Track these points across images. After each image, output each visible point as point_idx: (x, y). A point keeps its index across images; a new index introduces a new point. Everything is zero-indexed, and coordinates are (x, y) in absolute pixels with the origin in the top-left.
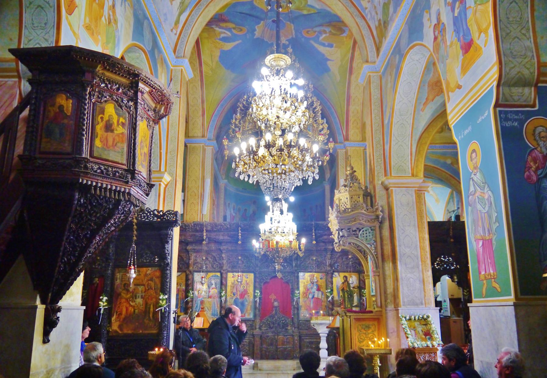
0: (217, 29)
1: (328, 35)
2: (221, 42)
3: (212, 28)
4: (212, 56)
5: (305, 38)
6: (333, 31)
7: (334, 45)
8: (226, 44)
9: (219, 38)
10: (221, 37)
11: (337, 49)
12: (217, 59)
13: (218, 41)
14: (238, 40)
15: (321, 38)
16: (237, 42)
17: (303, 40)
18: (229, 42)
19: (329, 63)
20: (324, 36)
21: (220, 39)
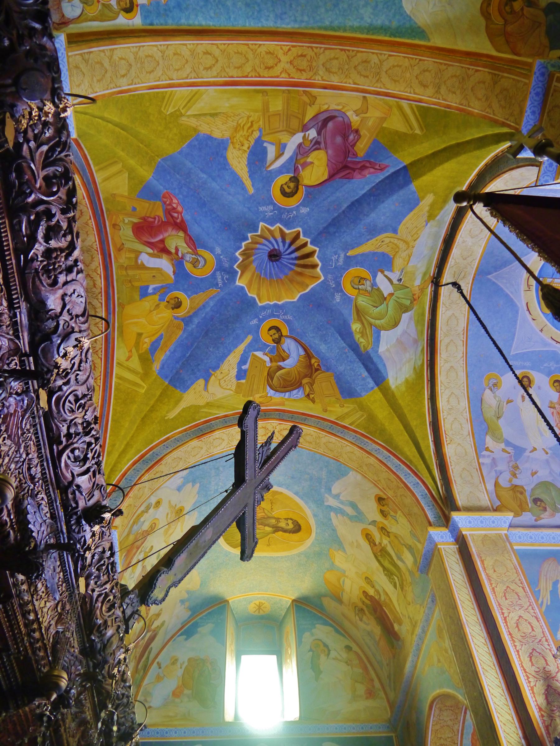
0: (298, 138)
1: (268, 364)
2: (252, 143)
3: (305, 128)
4: (213, 115)
5: (258, 327)
6: (280, 372)
7: (243, 381)
8: (246, 155)
9: (263, 139)
10: (265, 145)
11: (234, 388)
12: (205, 128)
13: (256, 134)
14: (253, 186)
15: (259, 354)
16: (248, 183)
17: (255, 321)
19: (201, 382)
20: (267, 359)
21: (259, 142)
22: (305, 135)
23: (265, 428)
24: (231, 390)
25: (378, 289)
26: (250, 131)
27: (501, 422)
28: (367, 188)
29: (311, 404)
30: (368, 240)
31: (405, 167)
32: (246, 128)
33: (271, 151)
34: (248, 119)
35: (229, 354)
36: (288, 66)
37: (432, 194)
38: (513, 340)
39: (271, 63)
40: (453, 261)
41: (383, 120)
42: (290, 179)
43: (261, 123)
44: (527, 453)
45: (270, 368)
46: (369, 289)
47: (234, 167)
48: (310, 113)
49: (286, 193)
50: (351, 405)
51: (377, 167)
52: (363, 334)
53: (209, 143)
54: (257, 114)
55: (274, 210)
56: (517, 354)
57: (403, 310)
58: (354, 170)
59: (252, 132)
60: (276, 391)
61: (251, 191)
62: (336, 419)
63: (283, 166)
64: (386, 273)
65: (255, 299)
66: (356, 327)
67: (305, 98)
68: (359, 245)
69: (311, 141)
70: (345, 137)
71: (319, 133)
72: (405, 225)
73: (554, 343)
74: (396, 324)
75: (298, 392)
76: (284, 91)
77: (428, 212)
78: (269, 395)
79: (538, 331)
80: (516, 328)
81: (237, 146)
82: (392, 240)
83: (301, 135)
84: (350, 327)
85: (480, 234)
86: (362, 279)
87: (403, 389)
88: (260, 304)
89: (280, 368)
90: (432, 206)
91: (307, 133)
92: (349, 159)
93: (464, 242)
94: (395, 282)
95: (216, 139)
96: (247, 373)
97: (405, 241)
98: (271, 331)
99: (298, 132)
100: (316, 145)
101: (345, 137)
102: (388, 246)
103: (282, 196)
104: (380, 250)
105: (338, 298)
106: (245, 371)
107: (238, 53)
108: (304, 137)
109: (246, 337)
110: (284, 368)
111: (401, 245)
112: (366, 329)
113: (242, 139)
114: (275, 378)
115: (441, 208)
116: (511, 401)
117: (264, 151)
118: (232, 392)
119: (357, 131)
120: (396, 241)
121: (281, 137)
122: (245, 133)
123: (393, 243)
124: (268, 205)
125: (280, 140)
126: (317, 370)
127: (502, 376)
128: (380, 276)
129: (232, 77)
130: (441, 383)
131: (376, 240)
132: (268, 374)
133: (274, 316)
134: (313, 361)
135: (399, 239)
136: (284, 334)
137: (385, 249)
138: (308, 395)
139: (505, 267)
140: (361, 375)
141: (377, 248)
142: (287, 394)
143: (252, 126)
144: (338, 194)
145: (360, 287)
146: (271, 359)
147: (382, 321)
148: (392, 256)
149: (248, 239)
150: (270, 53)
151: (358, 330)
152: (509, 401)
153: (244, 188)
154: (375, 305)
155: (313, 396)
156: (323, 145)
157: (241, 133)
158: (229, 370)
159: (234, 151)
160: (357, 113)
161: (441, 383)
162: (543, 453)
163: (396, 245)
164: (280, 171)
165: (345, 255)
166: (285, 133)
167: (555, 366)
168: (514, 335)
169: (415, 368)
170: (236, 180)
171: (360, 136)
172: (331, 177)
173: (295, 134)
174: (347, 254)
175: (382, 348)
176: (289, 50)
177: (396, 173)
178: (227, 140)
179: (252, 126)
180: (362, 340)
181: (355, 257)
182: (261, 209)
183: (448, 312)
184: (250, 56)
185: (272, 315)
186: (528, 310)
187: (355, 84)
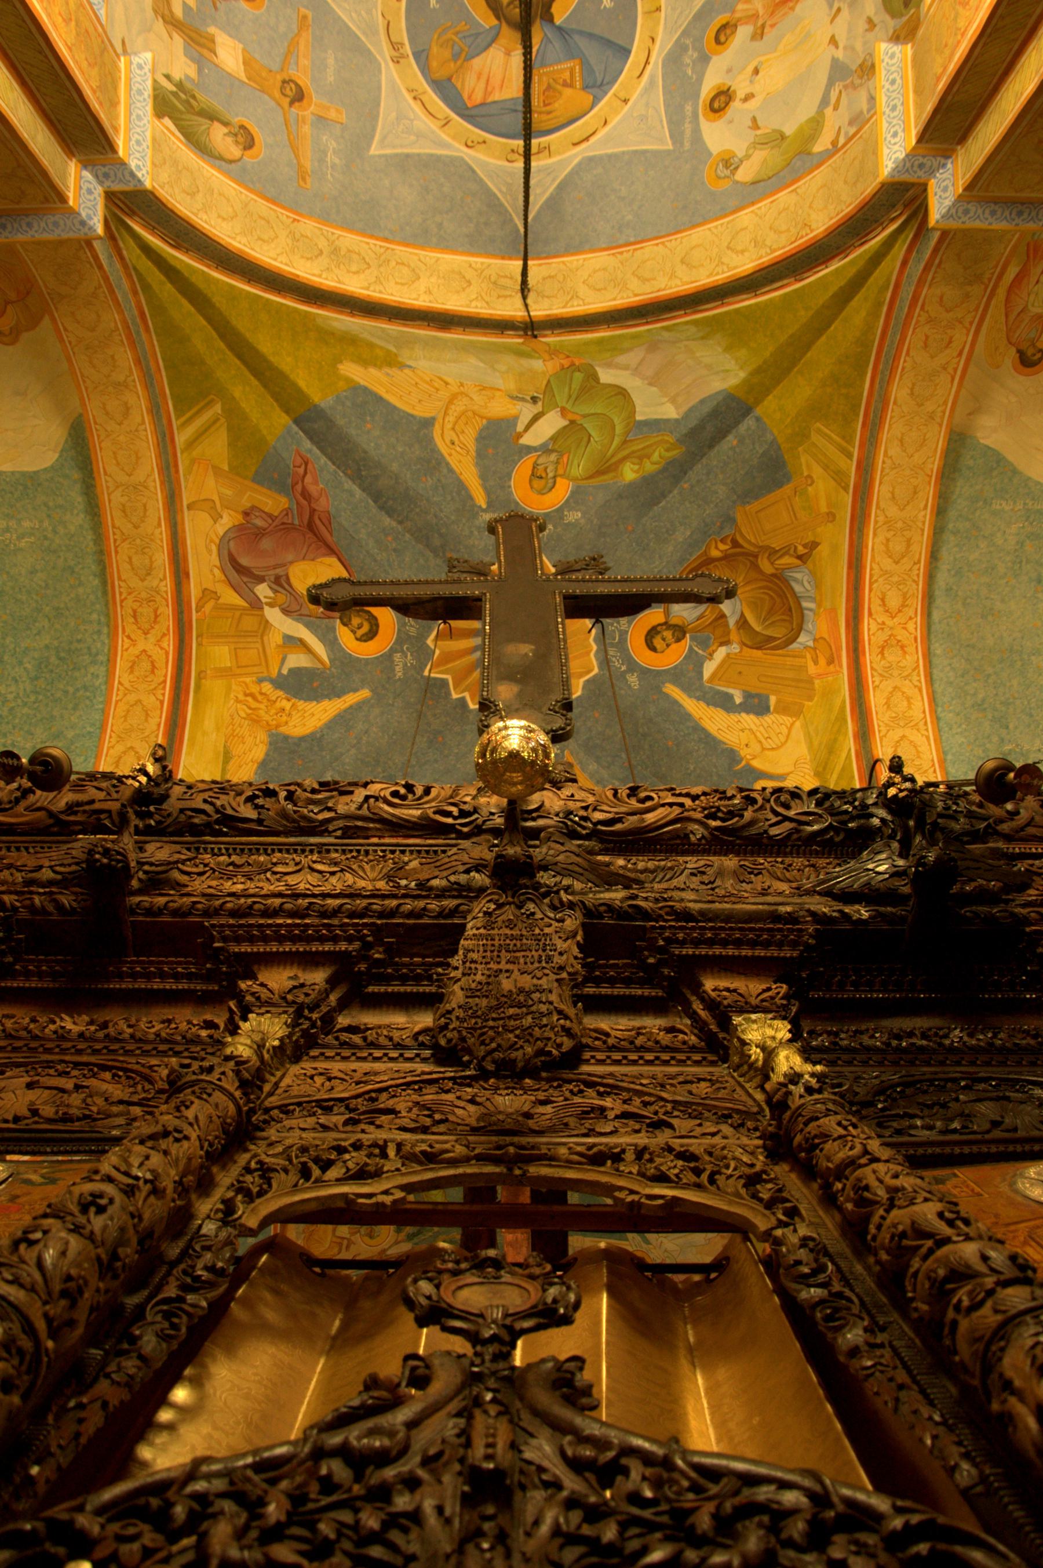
0: (273, 615)
1: (735, 648)
2: (280, 693)
3: (256, 605)
5: (645, 673)
7: (773, 700)
8: (301, 704)
9: (274, 673)
10: (285, 672)
11: (787, 720)
13: (267, 687)
14: (356, 690)
15: (709, 668)
16: (351, 699)
17: (633, 680)
18: (316, 696)
20: (721, 653)
21: (280, 683)
22: (267, 604)
23: (883, 648)
24: (792, 725)
25: (554, 438)
26: (260, 697)
27: (789, 130)
28: (348, 484)
29: (823, 550)
30: (451, 471)
31: (297, 421)
32: (254, 704)
33: (297, 660)
34: (240, 702)
35: (704, 730)
36: (152, 638)
37: (340, 367)
38: (644, 152)
39: (146, 665)
40: (474, 304)
41: (217, 471)
42: (345, 625)
43: (248, 680)
44: (840, 54)
45: (743, 644)
46: (553, 457)
47: (319, 724)
48: (230, 597)
49: (370, 631)
50: (803, 460)
51: (301, 470)
52: (641, 457)
53: (272, 765)
54: (234, 687)
55: (402, 651)
56: (671, 137)
57: (594, 383)
58: (313, 511)
59: (261, 694)
60: (800, 629)
61: (365, 693)
62: (846, 489)
63: (322, 639)
64: (520, 428)
65: (588, 681)
66: (629, 473)
67: (208, 607)
68: (461, 486)
69: (275, 591)
70: (260, 534)
71: (261, 580)
72: (414, 407)
73: (649, 68)
74: (621, 393)
75: (796, 580)
76: (199, 645)
77: (380, 368)
78: (811, 644)
79: (627, 108)
80: (623, 153)
81: (284, 718)
82: (449, 426)
83: (267, 611)
84: (632, 484)
85: (409, 266)
86: (535, 475)
87: (743, 353)
88: (596, 670)
89: (743, 623)
90: (365, 362)
91: (264, 600)
92: (296, 522)
93: (429, 292)
94: (539, 407)
95: (267, 755)
96: (754, 691)
97: (451, 402)
98: (658, 647)
99: (263, 616)
100: (281, 583)
101: (260, 534)
102: (463, 432)
103: (377, 638)
104: (472, 446)
105: (573, 516)
106: (748, 695)
107: (125, 717)
108: (271, 605)
109: (667, 696)
110: (742, 615)
111: (458, 407)
112: (633, 452)
113: (273, 711)
114: (769, 632)
115: (371, 346)
116: (754, 120)
117: (295, 672)
118: (798, 724)
119: (246, 514)
120: (451, 419)
121: (273, 645)
122: (262, 706)
123: (456, 423)
124: (393, 661)
125: (278, 646)
126: (735, 544)
127: (710, 154)
128: (527, 440)
129: (159, 725)
130: (710, 275)
131: (450, 455)
132: (758, 648)
133: (623, 641)
134: (715, 553)
135: (446, 414)
136: (662, 620)
137: (469, 438)
138: (800, 557)
139: (502, 205)
140: (732, 448)
141: (468, 452)
142: (805, 604)
143: (252, 696)
144: (363, 535)
145: (551, 475)
146: (722, 644)
147: (616, 421)
148: (485, 421)
149: (463, 700)
150: (132, 667)
151: (636, 467)
152: (755, 125)
153: (358, 707)
154: (585, 439)
155: (800, 548)
156: (279, 571)
157: (262, 713)
158: (742, 730)
159: (291, 724)
160: (216, 518)
161: (710, 275)
162: (838, 20)
163: (459, 418)
164: (331, 642)
165: (484, 511)
166: (265, 638)
167: (690, 52)
168: (635, 152)
169: (702, 338)
170: (342, 720)
171: (253, 508)
172: (331, 551)
173: (267, 622)
174: (484, 506)
175: (671, 412)
176: (129, 637)
177: (311, 435)
178: (271, 735)
179: (252, 695)
180: (656, 457)
181: (488, 492)
182: (399, 674)
183: (581, 294)
184: (132, 698)
185: (622, 645)
186: (587, 139)
187: (159, 525)
